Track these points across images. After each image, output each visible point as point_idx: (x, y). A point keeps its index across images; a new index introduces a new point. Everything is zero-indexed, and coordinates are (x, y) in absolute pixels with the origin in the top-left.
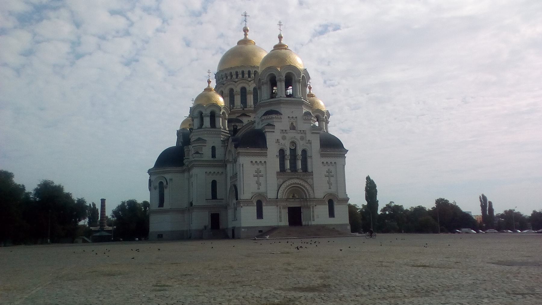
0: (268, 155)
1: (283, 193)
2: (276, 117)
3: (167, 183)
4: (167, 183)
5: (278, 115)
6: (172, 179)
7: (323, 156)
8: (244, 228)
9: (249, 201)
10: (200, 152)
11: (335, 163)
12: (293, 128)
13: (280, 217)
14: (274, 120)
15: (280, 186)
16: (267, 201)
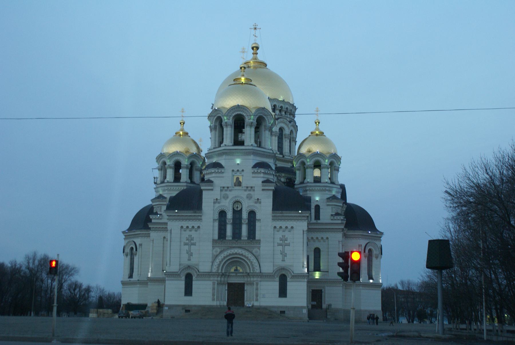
0: (203, 219)
1: (219, 265)
2: (215, 171)
3: (136, 250)
4: (136, 250)
5: (218, 169)
6: (142, 244)
7: (274, 218)
8: (167, 306)
9: (176, 274)
10: (159, 213)
11: (292, 227)
12: (238, 183)
13: (213, 295)
14: (214, 175)
15: (215, 257)
16: (198, 275)
